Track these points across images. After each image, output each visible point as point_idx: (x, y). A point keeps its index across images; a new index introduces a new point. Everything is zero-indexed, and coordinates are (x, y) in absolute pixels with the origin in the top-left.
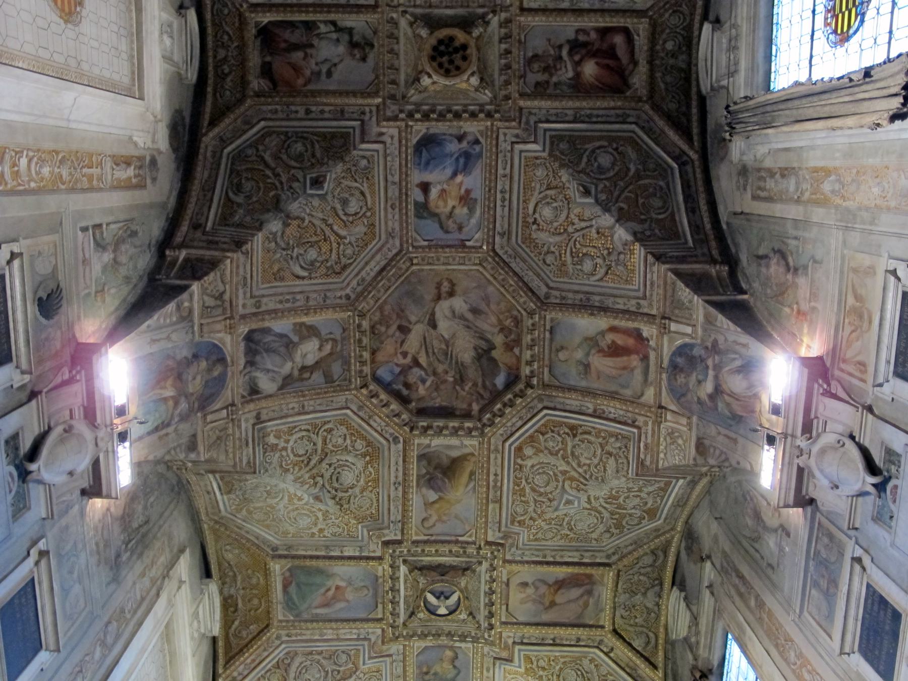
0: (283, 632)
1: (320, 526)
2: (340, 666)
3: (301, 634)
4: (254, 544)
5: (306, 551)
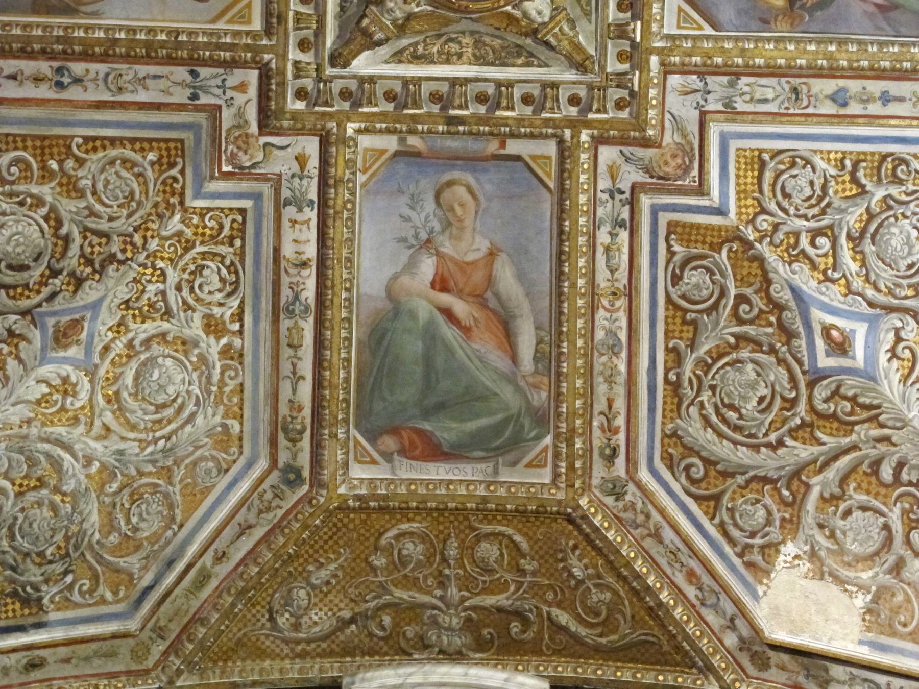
0: (599, 471)
1: (196, 329)
2: (723, 293)
3: (609, 414)
4: (266, 539)
5: (297, 378)
